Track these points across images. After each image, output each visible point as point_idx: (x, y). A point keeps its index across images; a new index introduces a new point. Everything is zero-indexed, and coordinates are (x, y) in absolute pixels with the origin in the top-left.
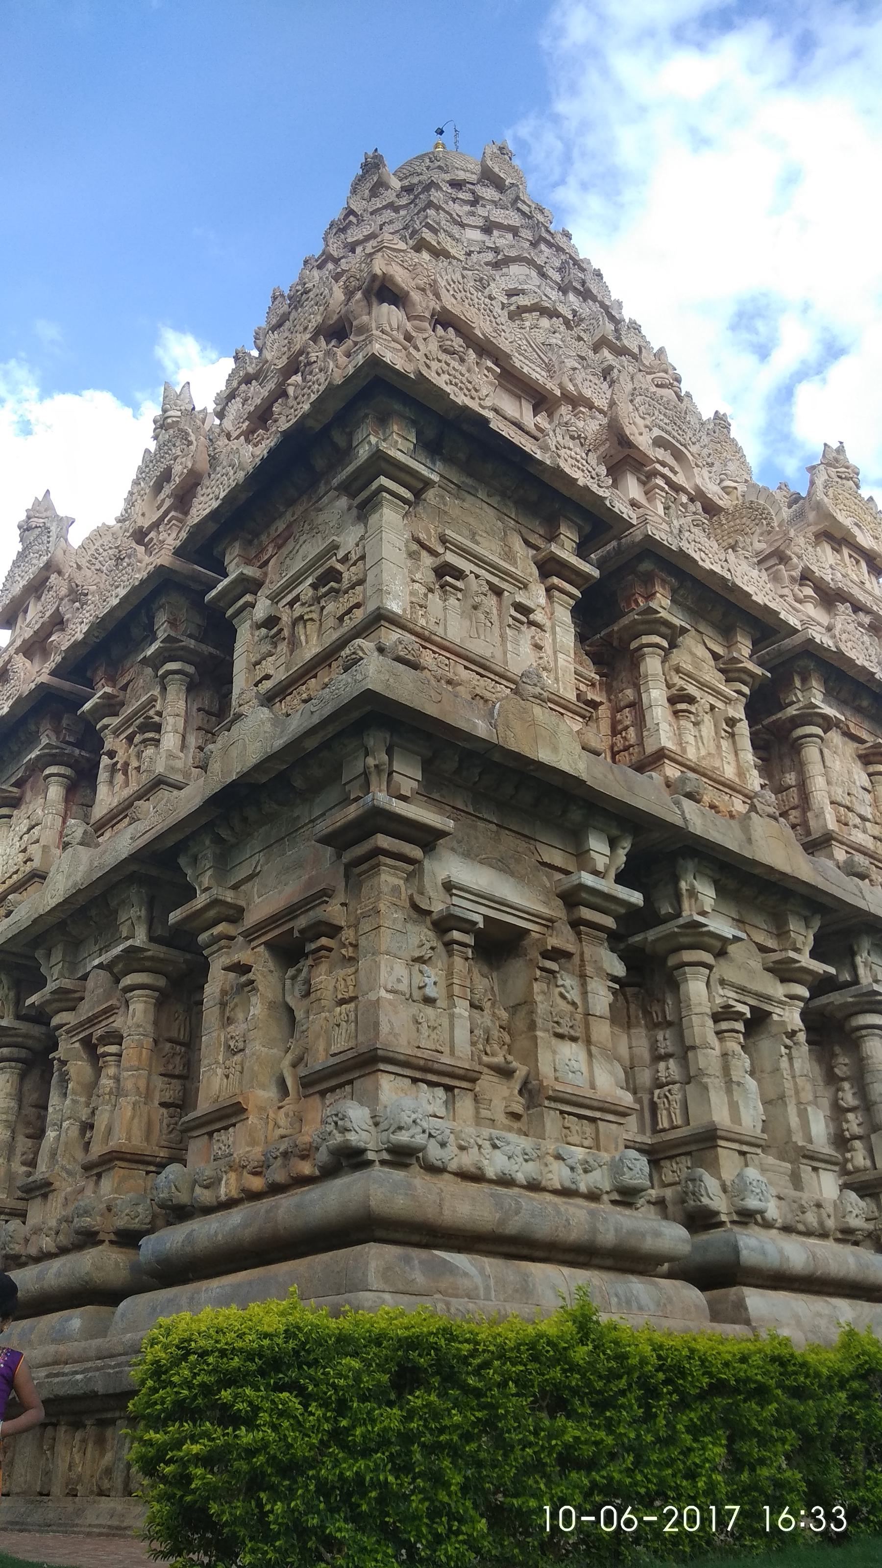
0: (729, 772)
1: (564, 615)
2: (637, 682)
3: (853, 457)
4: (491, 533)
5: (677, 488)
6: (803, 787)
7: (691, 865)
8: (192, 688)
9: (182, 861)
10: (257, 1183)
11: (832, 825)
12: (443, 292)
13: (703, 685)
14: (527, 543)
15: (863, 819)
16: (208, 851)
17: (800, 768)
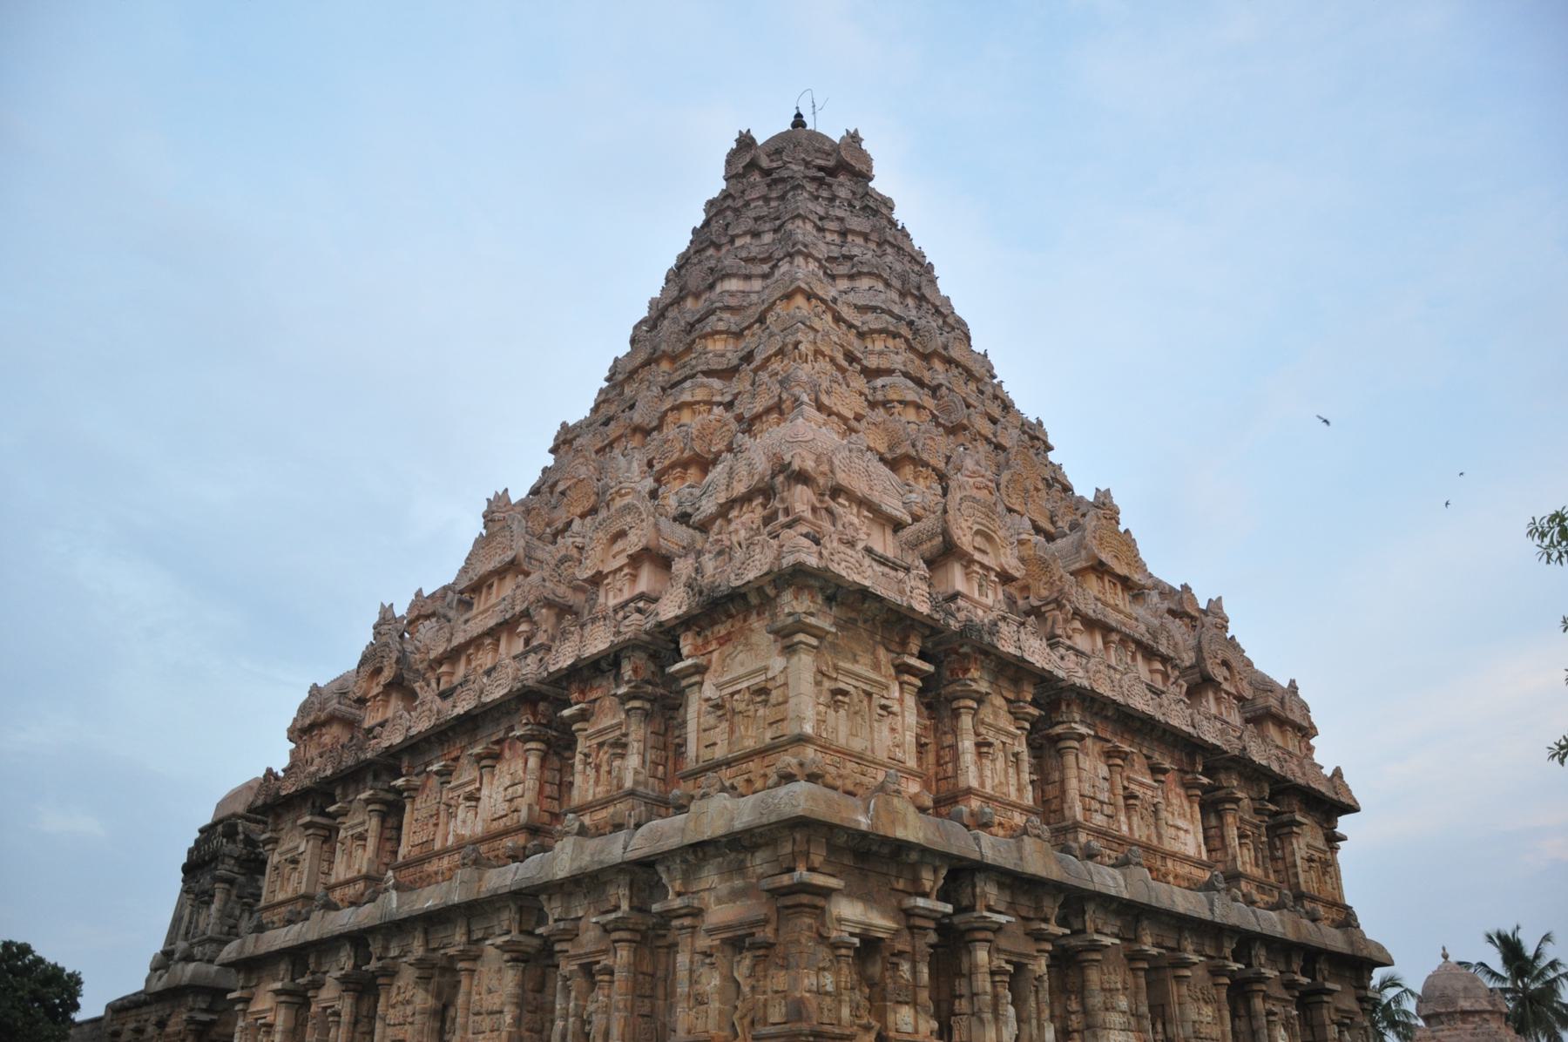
0: (1013, 796)
1: (910, 701)
2: (955, 731)
3: (1117, 500)
4: (866, 651)
5: (987, 568)
6: (1063, 781)
8: (647, 716)
9: (660, 869)
11: (1079, 817)
12: (837, 470)
13: (999, 730)
14: (888, 650)
15: (1102, 803)
16: (677, 866)
17: (1062, 769)
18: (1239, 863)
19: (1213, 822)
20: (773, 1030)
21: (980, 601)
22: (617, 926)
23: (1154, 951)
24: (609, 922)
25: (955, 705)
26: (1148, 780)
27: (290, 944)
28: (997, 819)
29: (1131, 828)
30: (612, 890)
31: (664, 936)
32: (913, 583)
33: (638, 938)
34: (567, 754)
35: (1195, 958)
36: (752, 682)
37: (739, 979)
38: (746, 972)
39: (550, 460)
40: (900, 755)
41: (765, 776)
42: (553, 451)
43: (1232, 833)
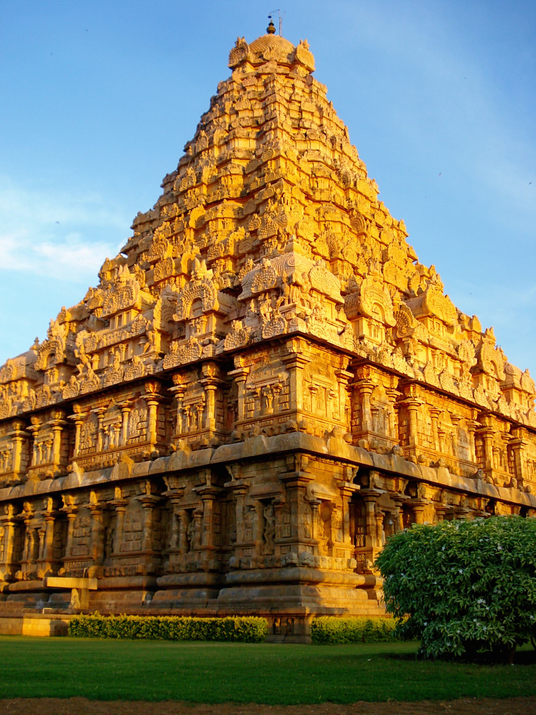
7: (373, 472)
10: (262, 566)
18: (492, 464)
19: (481, 443)
20: (285, 540)
21: (375, 340)
22: (205, 492)
23: (449, 507)
24: (202, 491)
25: (361, 391)
26: (450, 425)
27: (13, 497)
28: (380, 445)
29: (440, 449)
30: (201, 476)
31: (226, 497)
32: (346, 336)
33: (214, 498)
34: (168, 407)
35: (467, 510)
36: (272, 383)
37: (267, 518)
38: (270, 514)
39: (131, 233)
40: (337, 417)
41: (280, 427)
42: (134, 227)
43: (490, 449)
